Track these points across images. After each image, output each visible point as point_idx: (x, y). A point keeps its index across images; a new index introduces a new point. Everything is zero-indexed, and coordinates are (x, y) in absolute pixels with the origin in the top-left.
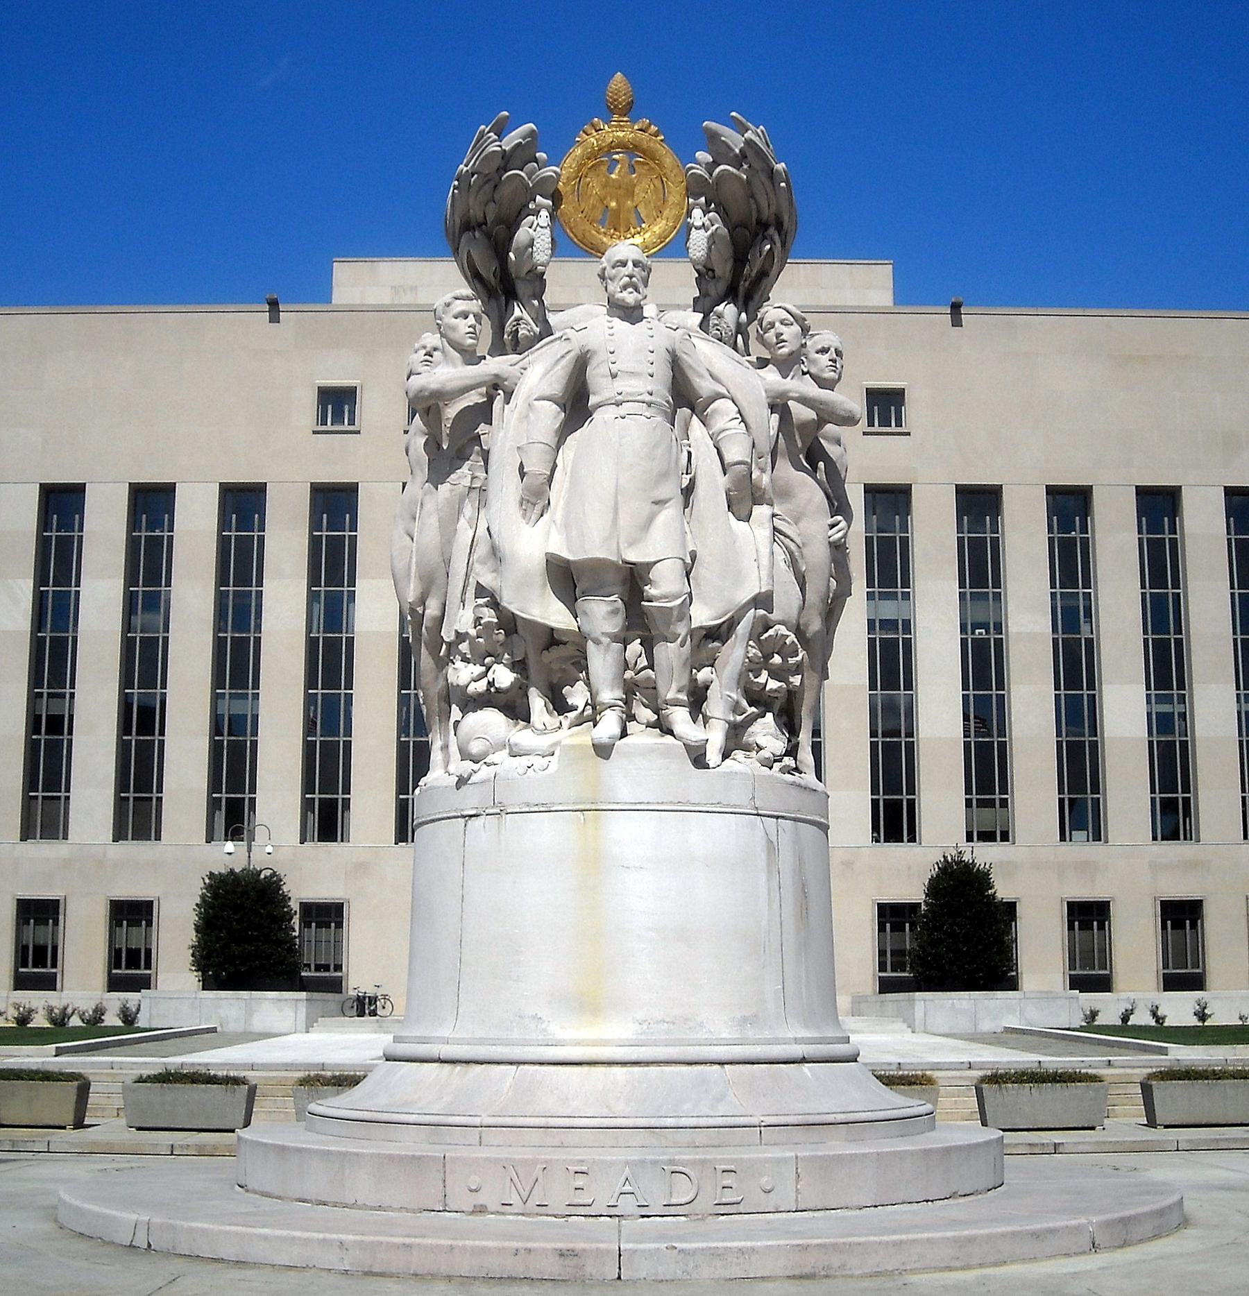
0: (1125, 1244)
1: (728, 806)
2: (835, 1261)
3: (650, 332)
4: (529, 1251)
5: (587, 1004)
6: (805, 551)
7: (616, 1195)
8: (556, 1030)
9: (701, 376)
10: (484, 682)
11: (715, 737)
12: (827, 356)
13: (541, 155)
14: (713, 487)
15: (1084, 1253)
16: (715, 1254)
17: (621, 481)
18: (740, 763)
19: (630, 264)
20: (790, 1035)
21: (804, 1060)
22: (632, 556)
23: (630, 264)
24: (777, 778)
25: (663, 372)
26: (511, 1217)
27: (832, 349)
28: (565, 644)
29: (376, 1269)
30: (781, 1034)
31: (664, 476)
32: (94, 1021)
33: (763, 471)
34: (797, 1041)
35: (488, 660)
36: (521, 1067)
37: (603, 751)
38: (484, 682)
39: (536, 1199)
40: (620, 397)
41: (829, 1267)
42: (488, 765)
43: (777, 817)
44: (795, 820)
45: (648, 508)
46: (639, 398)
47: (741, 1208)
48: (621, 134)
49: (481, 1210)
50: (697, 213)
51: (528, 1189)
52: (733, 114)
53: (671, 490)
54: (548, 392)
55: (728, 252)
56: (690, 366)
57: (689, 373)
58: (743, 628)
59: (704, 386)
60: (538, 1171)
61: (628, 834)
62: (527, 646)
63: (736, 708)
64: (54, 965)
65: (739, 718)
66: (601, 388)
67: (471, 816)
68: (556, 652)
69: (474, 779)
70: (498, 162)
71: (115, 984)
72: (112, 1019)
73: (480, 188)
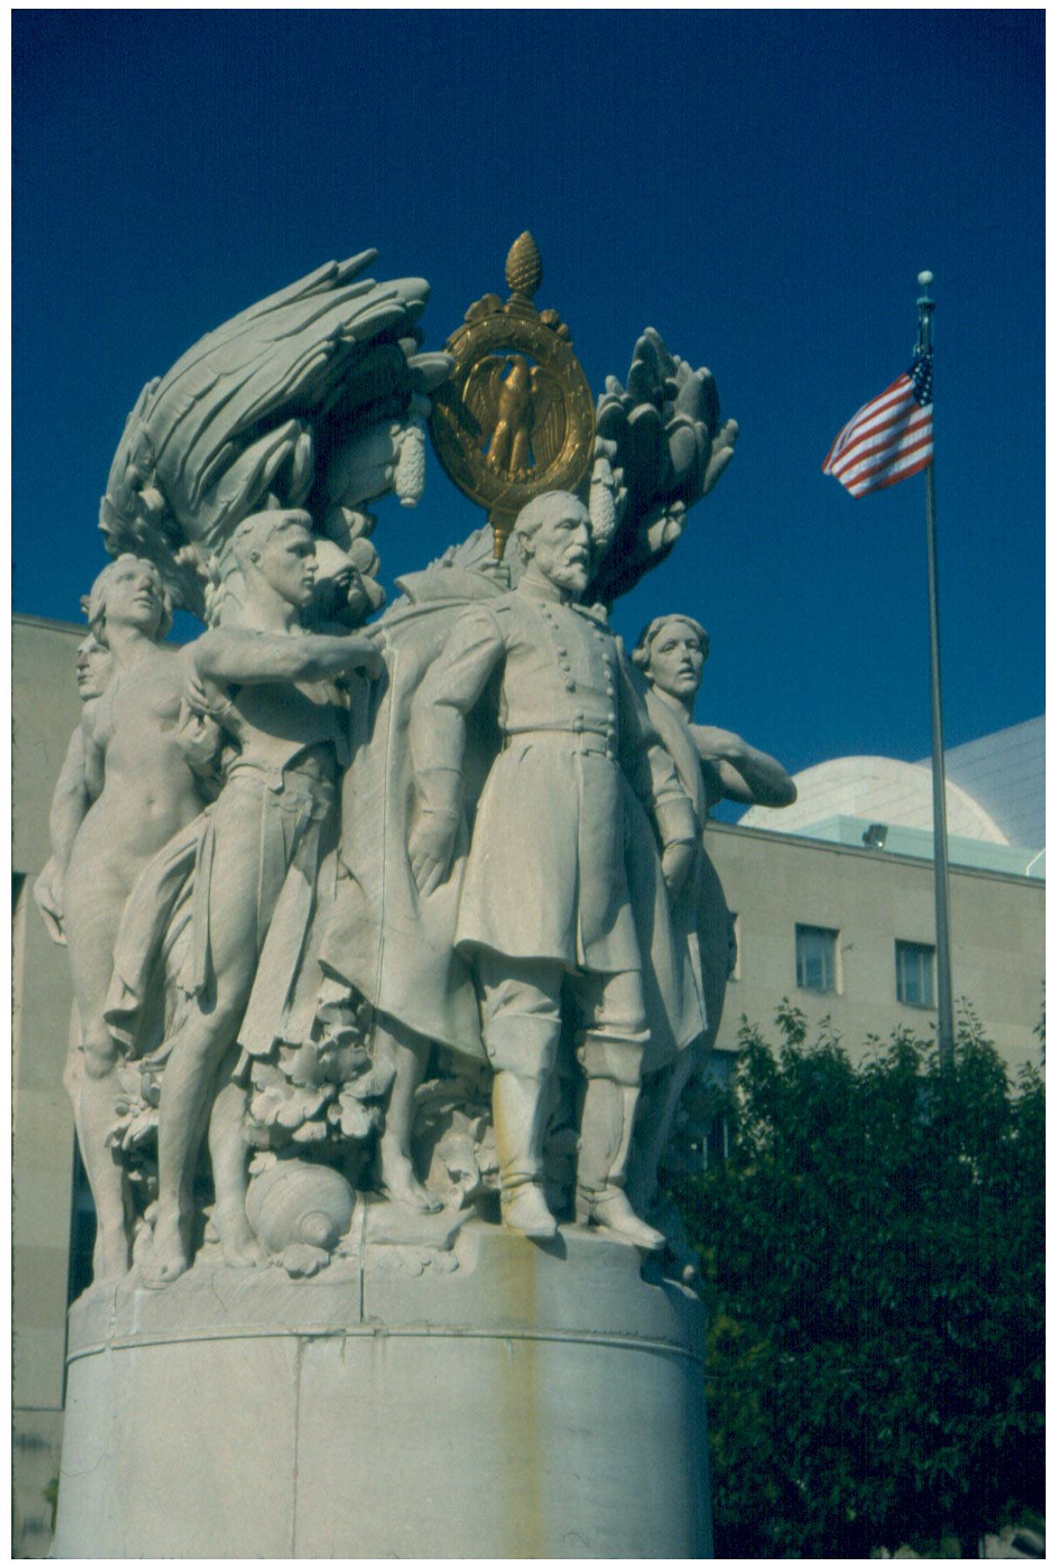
28: (454, 1077)
54: (458, 695)
67: (312, 1337)
69: (321, 1276)
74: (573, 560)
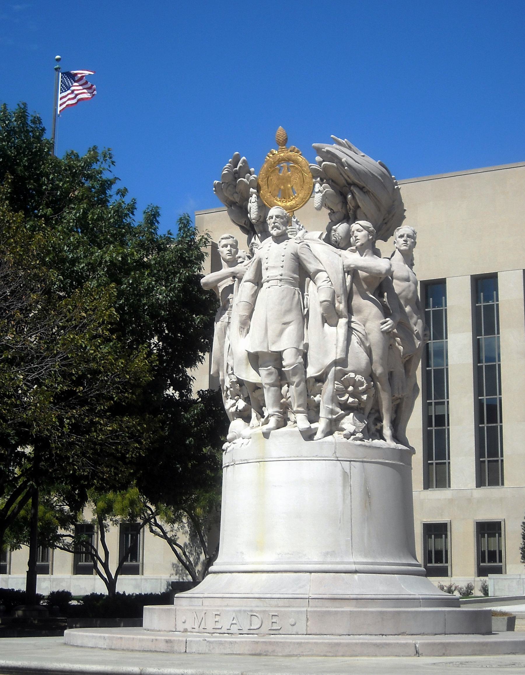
0: (444, 655)
1: (323, 457)
2: (270, 648)
3: (285, 247)
4: (156, 640)
5: (259, 546)
6: (370, 337)
7: (230, 625)
8: (248, 558)
9: (310, 263)
10: (235, 407)
11: (321, 425)
12: (403, 239)
13: (252, 169)
14: (316, 313)
15: (410, 656)
16: (221, 643)
17: (268, 316)
18: (337, 436)
19: (274, 217)
20: (352, 560)
21: (356, 572)
22: (274, 348)
23: (274, 217)
24: (349, 443)
25: (289, 263)
26: (195, 634)
27: (405, 235)
29: (113, 647)
30: (346, 560)
31: (288, 311)
32: (468, 592)
33: (340, 303)
34: (355, 563)
35: (236, 397)
36: (233, 574)
37: (266, 435)
38: (235, 407)
39: (202, 626)
40: (268, 279)
41: (267, 651)
42: (234, 443)
43: (350, 461)
44: (362, 462)
45: (280, 327)
46: (276, 278)
47: (280, 632)
48: (282, 155)
49: (186, 631)
50: (317, 185)
51: (200, 621)
52: (332, 136)
53: (293, 316)
55: (338, 199)
56: (305, 259)
57: (305, 262)
58: (331, 375)
59: (312, 267)
60: (203, 615)
61: (276, 472)
62: (246, 391)
63: (332, 412)
64: (447, 562)
65: (334, 417)
66: (265, 275)
68: (258, 392)
70: (231, 177)
71: (482, 572)
72: (477, 593)
73: (227, 188)
74: (273, 228)
